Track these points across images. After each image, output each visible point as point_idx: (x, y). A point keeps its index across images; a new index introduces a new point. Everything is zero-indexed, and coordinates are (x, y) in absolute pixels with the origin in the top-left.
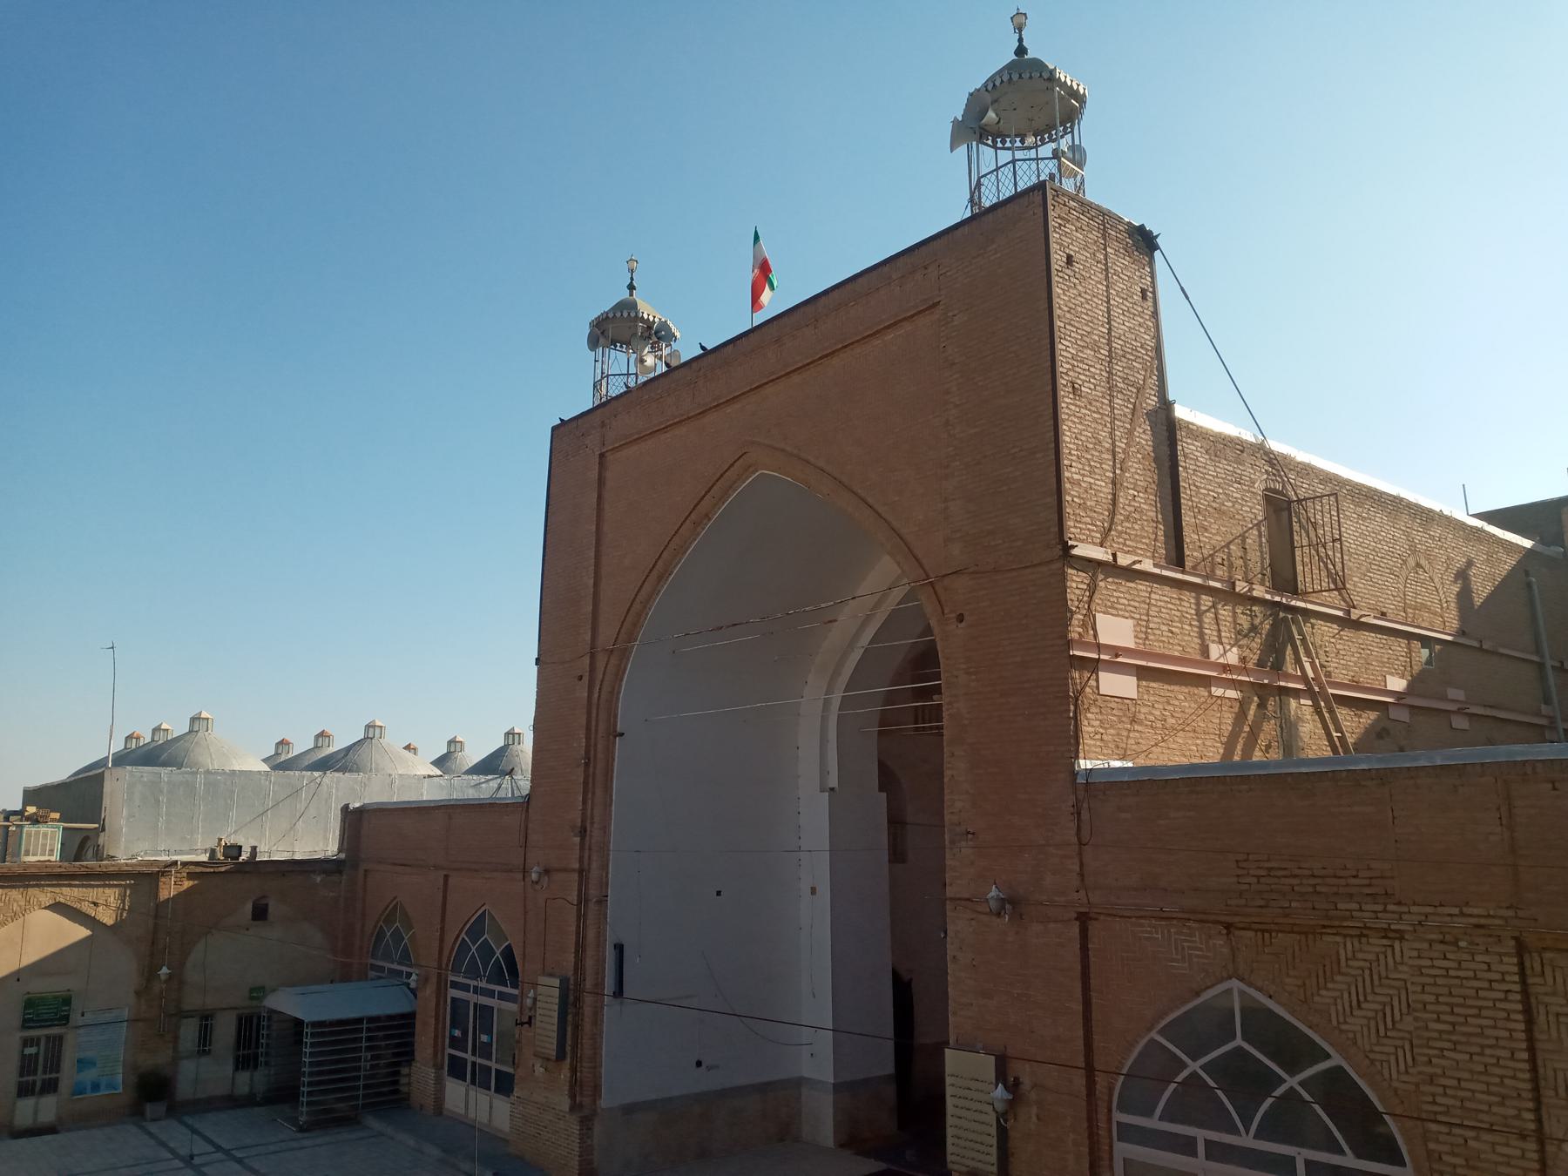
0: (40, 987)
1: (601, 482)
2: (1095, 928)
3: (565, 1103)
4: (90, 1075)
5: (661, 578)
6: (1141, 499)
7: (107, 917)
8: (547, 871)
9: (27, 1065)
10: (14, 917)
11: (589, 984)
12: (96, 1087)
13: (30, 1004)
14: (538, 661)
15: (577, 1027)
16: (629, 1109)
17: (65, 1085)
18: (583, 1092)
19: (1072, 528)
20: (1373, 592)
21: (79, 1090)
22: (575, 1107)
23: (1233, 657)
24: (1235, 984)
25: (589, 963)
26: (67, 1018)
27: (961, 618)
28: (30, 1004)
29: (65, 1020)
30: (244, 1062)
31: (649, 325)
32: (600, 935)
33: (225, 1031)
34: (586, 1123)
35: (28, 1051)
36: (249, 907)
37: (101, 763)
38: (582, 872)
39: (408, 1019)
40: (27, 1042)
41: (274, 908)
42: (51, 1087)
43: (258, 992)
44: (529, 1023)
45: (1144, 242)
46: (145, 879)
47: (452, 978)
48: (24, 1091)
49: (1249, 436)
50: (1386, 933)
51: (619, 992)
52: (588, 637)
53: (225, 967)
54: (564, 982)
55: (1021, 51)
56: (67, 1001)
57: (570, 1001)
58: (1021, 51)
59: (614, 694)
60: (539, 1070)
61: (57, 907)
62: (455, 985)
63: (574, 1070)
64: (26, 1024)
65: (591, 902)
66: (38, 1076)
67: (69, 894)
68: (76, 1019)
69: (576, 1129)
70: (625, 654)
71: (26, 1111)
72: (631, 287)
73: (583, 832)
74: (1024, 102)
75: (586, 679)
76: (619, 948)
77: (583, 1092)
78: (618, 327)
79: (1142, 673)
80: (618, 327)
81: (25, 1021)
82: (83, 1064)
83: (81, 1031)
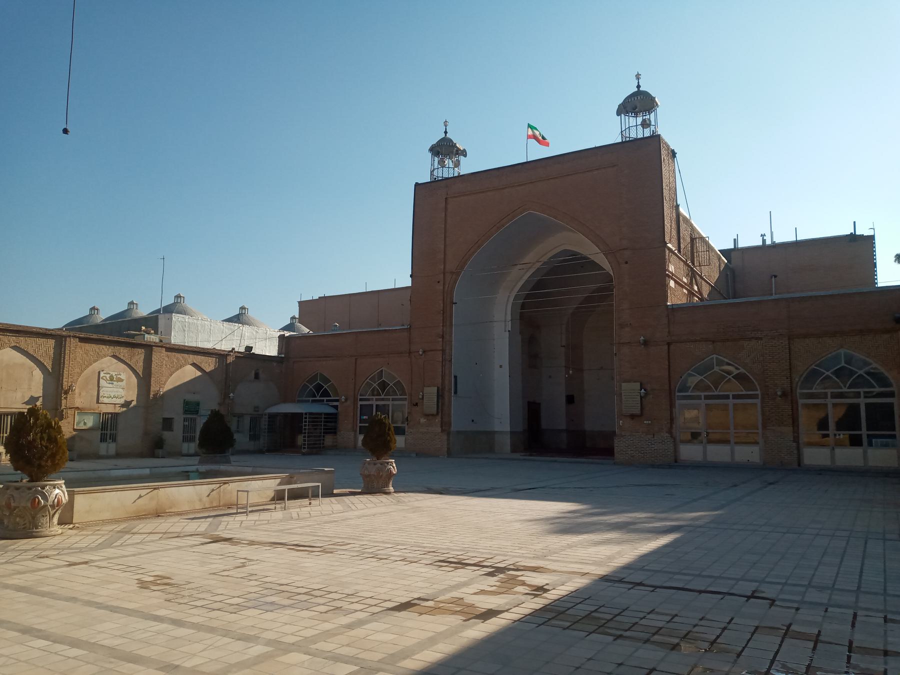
0: (190, 398)
1: (446, 208)
2: (672, 347)
3: (439, 430)
5: (479, 247)
6: (674, 233)
7: (208, 369)
8: (424, 352)
10: (181, 367)
11: (447, 388)
13: (186, 403)
14: (411, 276)
15: (443, 404)
16: (458, 432)
18: (445, 426)
19: (667, 239)
20: (705, 271)
22: (443, 431)
23: (685, 280)
24: (715, 356)
25: (447, 382)
27: (626, 263)
28: (186, 403)
29: (197, 412)
30: (254, 437)
31: (458, 149)
32: (450, 372)
33: (247, 421)
34: (449, 434)
36: (253, 372)
37: (158, 311)
38: (443, 351)
39: (332, 418)
41: (261, 375)
43: (256, 408)
44: (417, 404)
45: (673, 154)
46: (220, 356)
47: (359, 397)
49: (688, 216)
50: (757, 338)
51: (456, 392)
52: (442, 267)
53: (249, 396)
54: (438, 388)
55: (639, 86)
56: (198, 404)
57: (440, 395)
58: (639, 86)
59: (453, 288)
60: (423, 420)
62: (361, 400)
63: (442, 418)
65: (446, 361)
67: (198, 359)
69: (445, 437)
70: (458, 274)
72: (446, 132)
73: (443, 337)
74: (639, 103)
75: (442, 283)
76: (455, 377)
77: (445, 426)
78: (445, 149)
79: (676, 282)
80: (445, 149)
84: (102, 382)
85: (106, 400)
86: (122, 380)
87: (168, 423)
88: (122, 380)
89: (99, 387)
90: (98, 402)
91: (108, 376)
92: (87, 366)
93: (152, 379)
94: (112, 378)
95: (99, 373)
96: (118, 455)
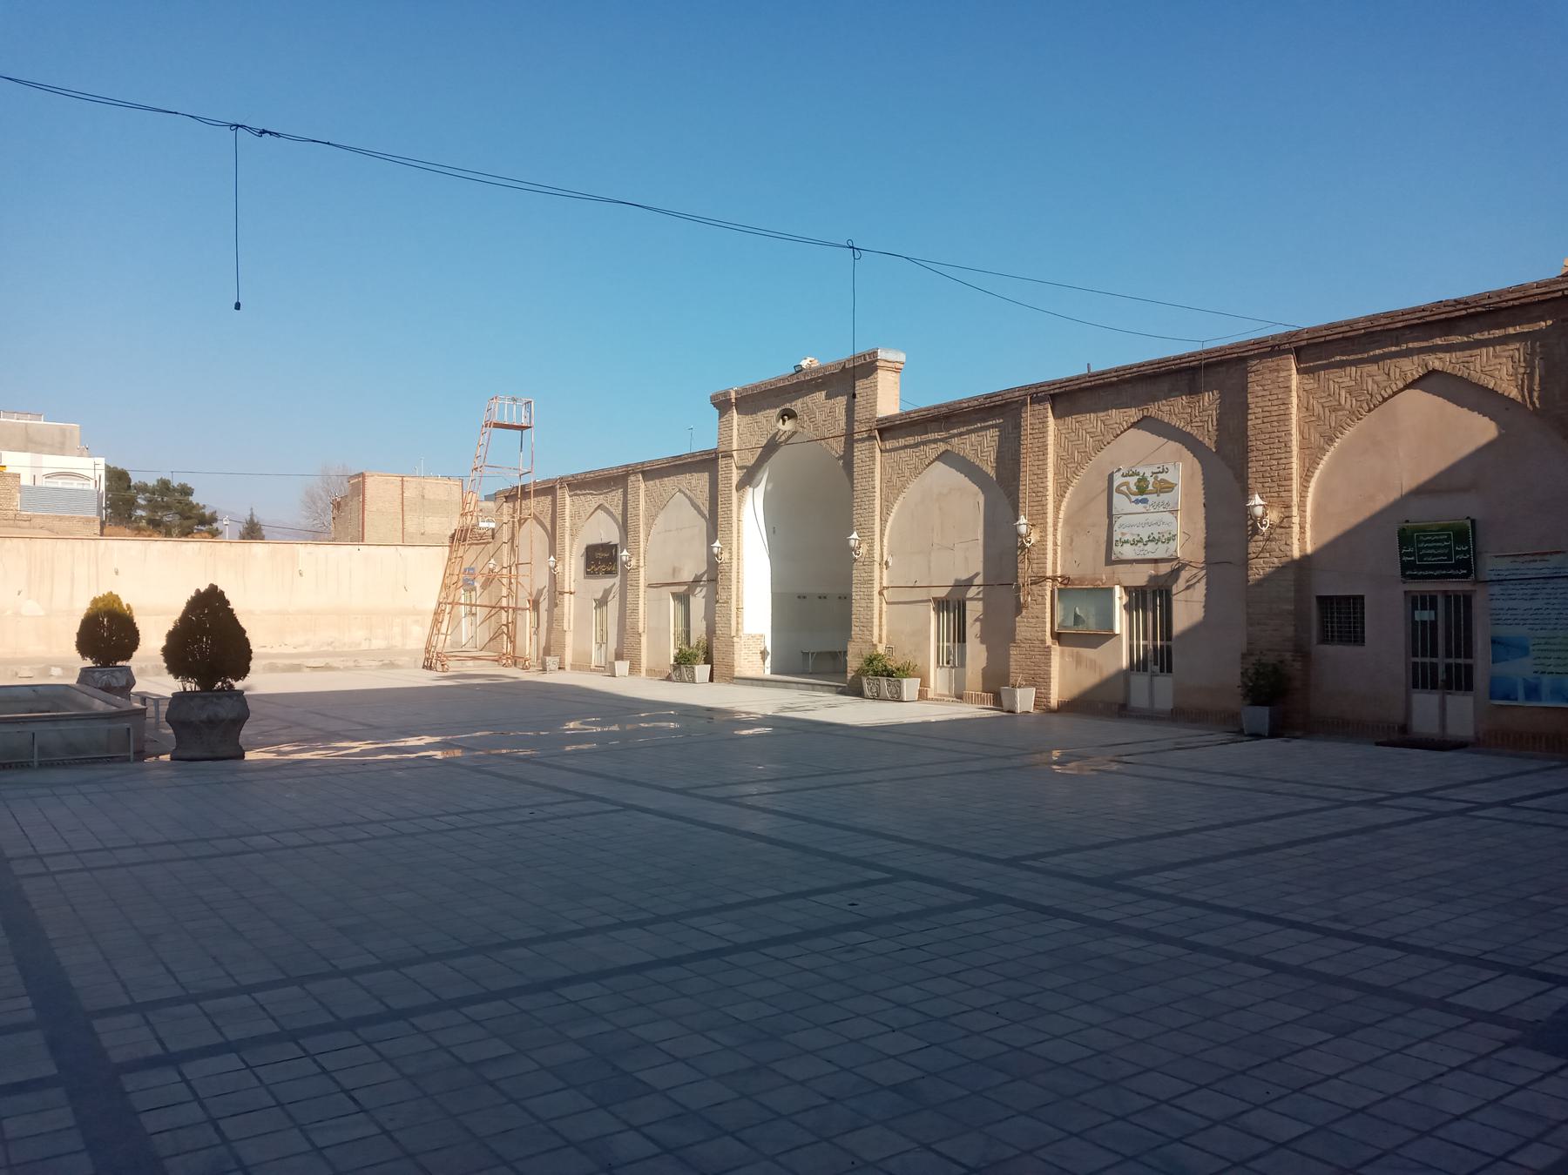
0: (1422, 515)
4: (1519, 669)
9: (1422, 638)
12: (1533, 691)
17: (1481, 679)
21: (1502, 690)
26: (1465, 564)
29: (1466, 567)
35: (1418, 615)
40: (1419, 601)
42: (1461, 680)
48: (1423, 679)
61: (1428, 381)
64: (1409, 570)
66: (1441, 655)
68: (1491, 564)
71: (1426, 709)
81: (1405, 566)
82: (1499, 644)
83: (1496, 589)
84: (1120, 502)
85: (1127, 552)
86: (1167, 487)
87: (1343, 617)
88: (1167, 487)
89: (1110, 515)
90: (1110, 561)
91: (1133, 480)
92: (1080, 465)
93: (1253, 467)
94: (1142, 489)
95: (1111, 478)
96: (1178, 715)
